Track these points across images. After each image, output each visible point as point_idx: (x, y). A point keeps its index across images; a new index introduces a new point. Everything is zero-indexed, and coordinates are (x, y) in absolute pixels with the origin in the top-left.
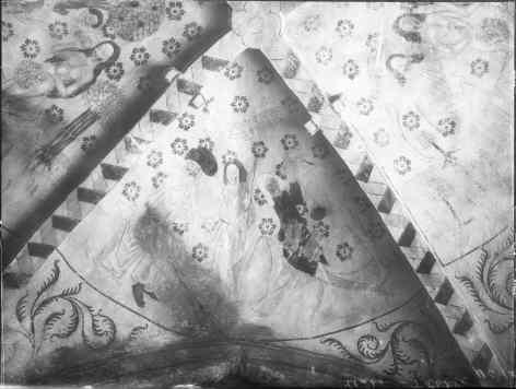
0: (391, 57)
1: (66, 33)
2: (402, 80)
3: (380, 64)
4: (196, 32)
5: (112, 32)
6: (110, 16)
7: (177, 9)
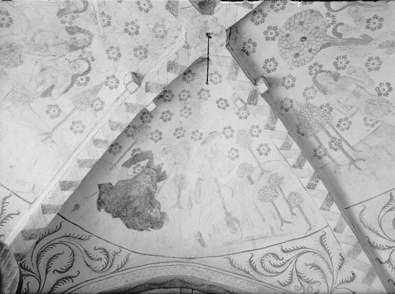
1: (368, 21)
4: (256, 17)
5: (328, 18)
6: (325, 31)
7: (269, 35)
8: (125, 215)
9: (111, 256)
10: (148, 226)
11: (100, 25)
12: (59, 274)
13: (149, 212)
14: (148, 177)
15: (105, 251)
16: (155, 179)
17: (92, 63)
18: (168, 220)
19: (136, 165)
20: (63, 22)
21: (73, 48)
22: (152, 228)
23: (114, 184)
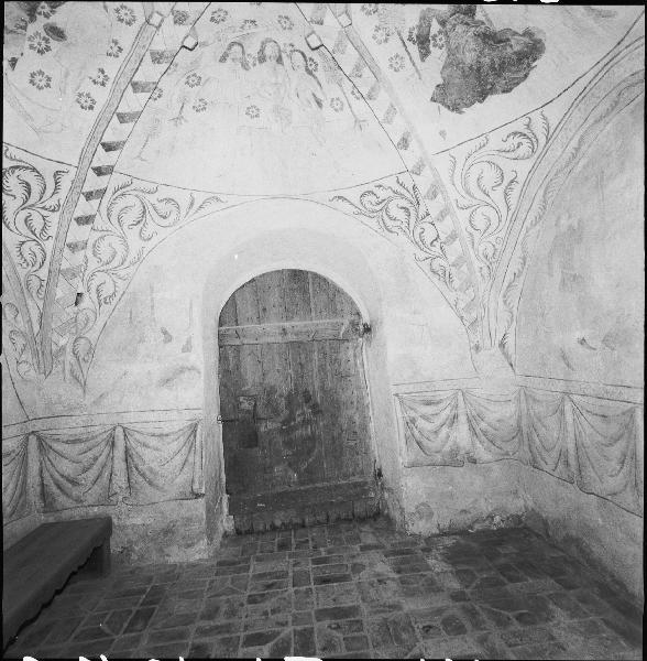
0: (240, 44)
2: (223, 59)
3: (232, 37)
8: (489, 87)
9: (526, 132)
10: (529, 65)
11: (254, 30)
12: (499, 188)
13: (509, 50)
14: (460, 29)
15: (515, 134)
16: (467, 19)
17: (297, 47)
18: (540, 31)
19: (432, 42)
20: (255, 65)
21: (279, 60)
22: (535, 60)
23: (440, 81)
